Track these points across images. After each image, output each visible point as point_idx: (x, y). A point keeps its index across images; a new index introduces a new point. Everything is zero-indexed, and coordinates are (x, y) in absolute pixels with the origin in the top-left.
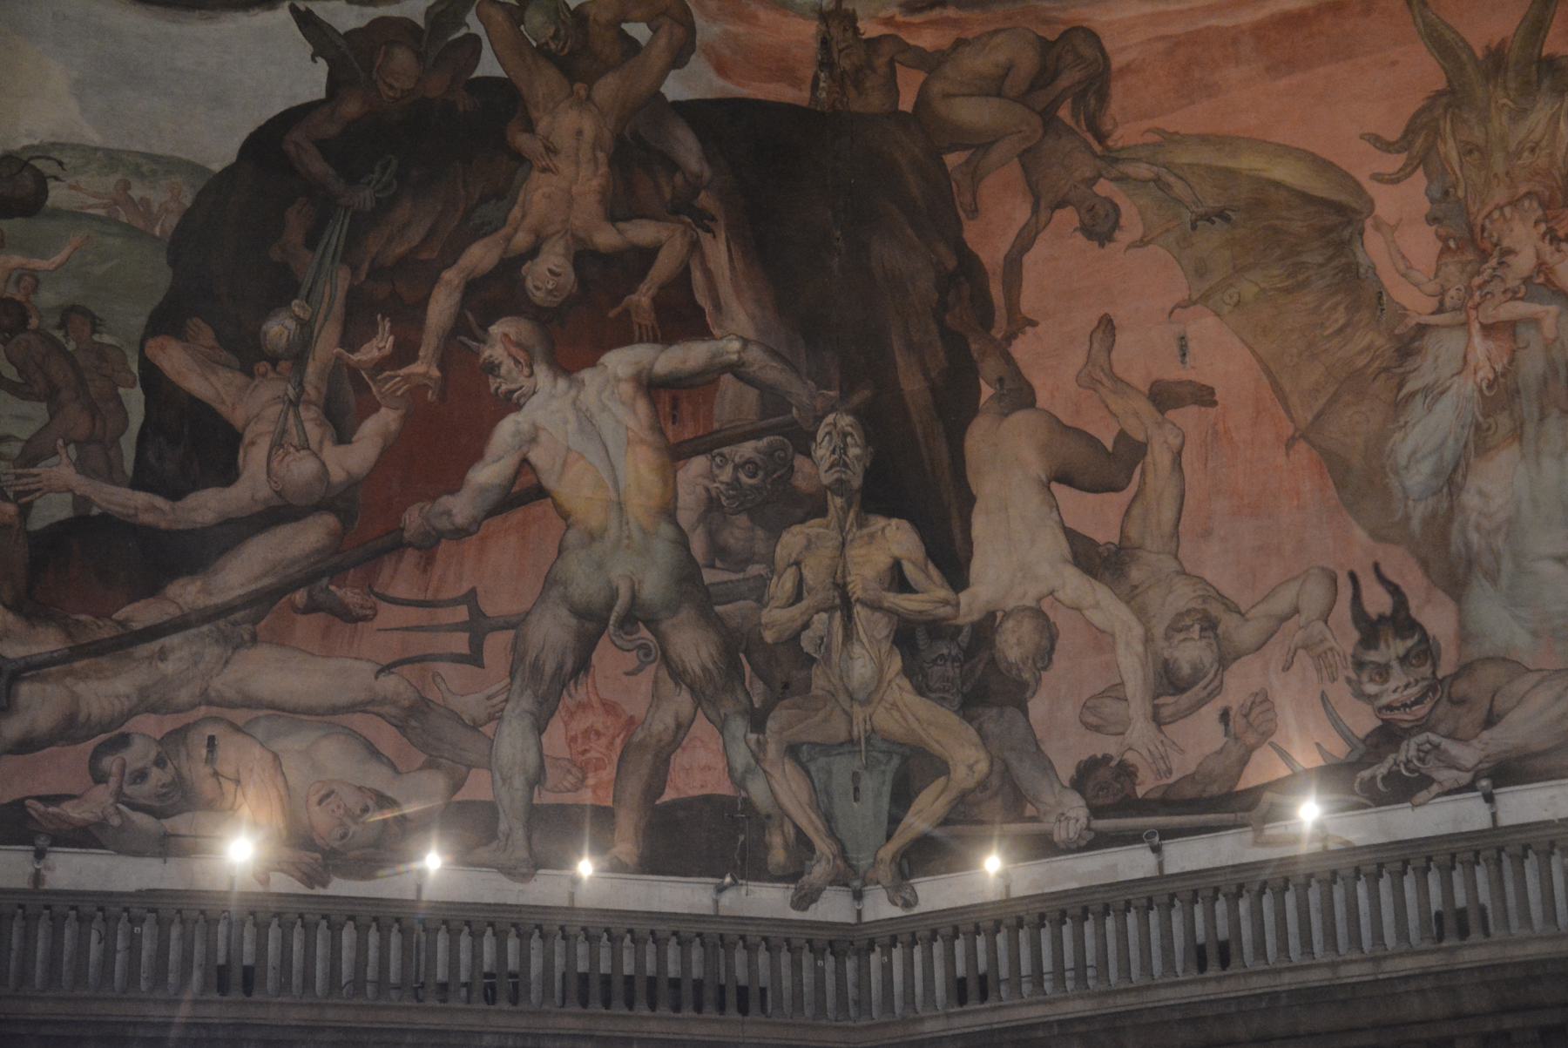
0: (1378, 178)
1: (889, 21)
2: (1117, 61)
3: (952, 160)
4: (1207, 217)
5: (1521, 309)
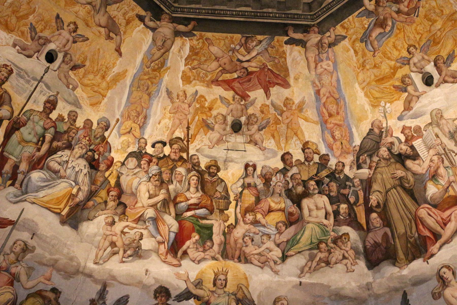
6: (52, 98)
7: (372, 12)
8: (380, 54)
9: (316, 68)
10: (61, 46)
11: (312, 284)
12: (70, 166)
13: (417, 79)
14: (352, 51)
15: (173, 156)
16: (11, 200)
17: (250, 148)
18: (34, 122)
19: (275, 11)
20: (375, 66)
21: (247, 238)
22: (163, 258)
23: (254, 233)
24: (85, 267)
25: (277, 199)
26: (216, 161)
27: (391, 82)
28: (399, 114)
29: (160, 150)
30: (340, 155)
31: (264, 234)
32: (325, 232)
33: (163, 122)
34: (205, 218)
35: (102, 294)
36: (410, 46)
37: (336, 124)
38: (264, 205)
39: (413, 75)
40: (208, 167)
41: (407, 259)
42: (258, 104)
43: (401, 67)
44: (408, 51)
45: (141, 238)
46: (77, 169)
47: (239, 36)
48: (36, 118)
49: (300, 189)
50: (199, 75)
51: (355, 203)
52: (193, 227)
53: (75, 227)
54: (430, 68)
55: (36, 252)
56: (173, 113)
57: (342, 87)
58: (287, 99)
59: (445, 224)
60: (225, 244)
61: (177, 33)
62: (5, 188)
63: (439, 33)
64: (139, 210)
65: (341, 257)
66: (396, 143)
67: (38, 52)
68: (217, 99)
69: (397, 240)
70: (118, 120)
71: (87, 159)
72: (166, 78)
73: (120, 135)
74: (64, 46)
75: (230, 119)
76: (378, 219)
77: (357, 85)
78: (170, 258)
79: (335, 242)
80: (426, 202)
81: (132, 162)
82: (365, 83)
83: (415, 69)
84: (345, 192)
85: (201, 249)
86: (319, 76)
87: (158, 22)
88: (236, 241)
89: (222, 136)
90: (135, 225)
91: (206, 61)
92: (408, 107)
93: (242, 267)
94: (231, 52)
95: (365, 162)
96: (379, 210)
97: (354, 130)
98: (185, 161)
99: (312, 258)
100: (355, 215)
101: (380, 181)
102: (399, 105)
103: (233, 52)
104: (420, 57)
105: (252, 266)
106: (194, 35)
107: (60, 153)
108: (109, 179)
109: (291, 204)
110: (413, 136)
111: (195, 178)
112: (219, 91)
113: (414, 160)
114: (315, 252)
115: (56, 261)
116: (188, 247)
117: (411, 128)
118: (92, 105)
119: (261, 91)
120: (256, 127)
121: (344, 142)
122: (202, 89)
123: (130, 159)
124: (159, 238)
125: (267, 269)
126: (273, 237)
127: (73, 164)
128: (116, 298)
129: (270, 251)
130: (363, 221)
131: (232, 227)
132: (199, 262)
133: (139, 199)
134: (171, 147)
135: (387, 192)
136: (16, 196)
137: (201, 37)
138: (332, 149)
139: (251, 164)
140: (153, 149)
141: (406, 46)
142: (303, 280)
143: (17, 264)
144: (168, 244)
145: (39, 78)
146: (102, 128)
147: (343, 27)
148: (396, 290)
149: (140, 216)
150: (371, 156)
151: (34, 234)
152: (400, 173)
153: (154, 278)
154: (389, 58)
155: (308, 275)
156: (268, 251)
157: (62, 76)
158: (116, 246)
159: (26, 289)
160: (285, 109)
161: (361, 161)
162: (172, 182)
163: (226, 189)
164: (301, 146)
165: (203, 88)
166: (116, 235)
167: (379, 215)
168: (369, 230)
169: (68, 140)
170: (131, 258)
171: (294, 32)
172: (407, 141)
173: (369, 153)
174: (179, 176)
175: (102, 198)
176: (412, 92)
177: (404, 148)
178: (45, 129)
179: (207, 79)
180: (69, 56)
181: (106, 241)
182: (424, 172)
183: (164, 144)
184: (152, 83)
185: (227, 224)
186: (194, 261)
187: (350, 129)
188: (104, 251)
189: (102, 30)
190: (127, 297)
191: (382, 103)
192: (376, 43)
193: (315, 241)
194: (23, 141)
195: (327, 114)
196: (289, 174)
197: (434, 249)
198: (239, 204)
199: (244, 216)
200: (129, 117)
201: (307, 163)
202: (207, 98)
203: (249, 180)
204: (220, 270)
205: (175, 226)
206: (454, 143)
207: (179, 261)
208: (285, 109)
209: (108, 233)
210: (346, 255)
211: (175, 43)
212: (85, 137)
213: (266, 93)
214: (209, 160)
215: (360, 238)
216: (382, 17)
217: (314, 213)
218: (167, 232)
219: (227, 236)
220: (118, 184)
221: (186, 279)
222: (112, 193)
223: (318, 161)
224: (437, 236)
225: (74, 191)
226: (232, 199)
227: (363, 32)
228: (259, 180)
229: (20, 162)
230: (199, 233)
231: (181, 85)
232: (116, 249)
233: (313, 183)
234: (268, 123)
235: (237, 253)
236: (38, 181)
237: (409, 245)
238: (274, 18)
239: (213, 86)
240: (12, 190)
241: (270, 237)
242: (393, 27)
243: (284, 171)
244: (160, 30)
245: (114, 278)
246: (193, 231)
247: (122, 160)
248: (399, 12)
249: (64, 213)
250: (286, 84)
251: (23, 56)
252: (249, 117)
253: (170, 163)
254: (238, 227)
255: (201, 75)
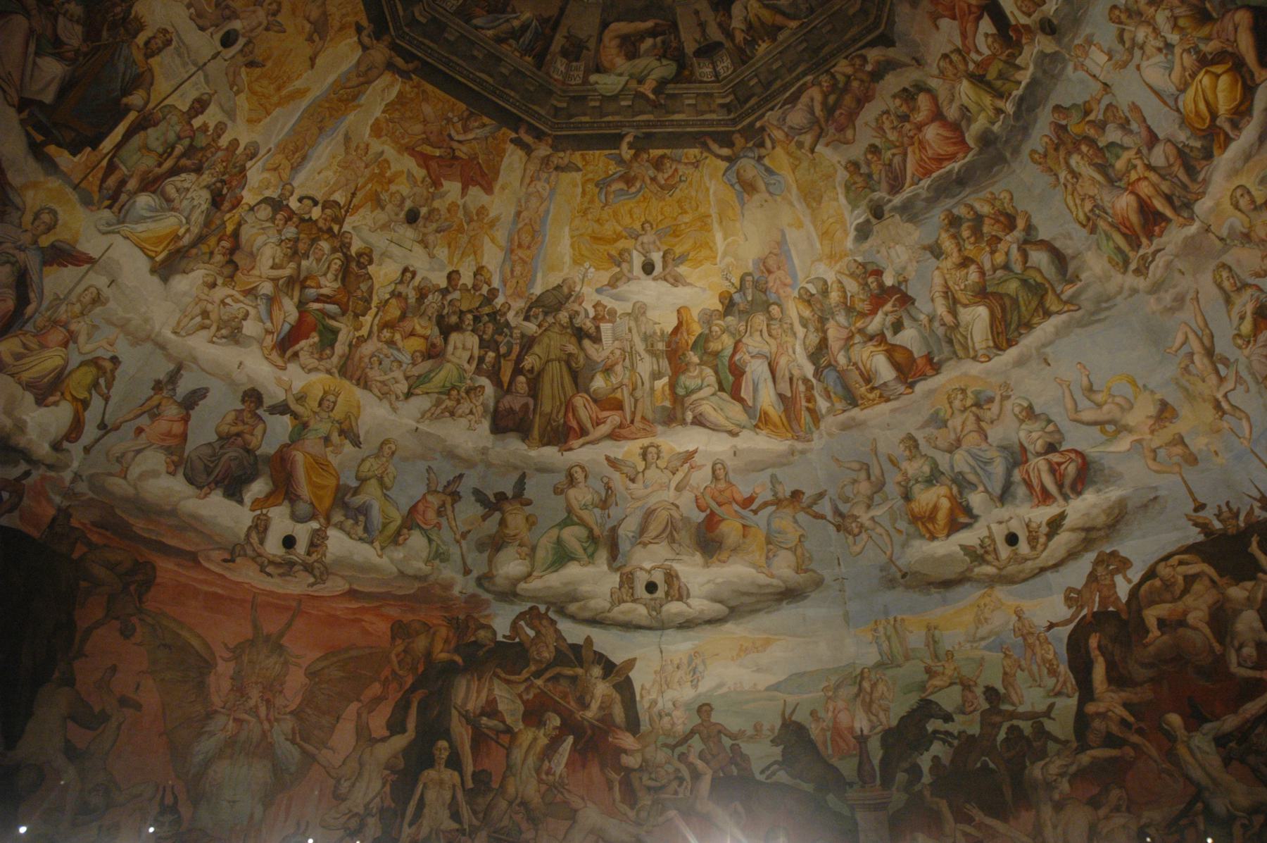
0: (221, 657)
1: (84, 525)
2: (158, 580)
3: (83, 584)
4: (165, 646)
5: (246, 716)
6: (205, 97)
7: (625, 162)
8: (610, 211)
9: (529, 184)
10: (248, 28)
11: (429, 434)
12: (189, 196)
13: (638, 260)
14: (580, 190)
15: (321, 224)
16: (101, 228)
17: (418, 249)
18: (169, 124)
19: (518, 98)
20: (598, 221)
21: (375, 358)
22: (266, 352)
23: (386, 356)
24: (159, 334)
25: (424, 322)
26: (371, 251)
27: (607, 248)
28: (599, 286)
29: (307, 208)
30: (510, 296)
31: (396, 360)
32: (462, 379)
33: (325, 174)
34: (333, 318)
35: (174, 377)
36: (647, 221)
37: (520, 258)
38: (407, 325)
39: (635, 253)
40: (360, 255)
41: (541, 441)
42: (450, 199)
43: (626, 238)
44: (642, 225)
45: (246, 315)
46: (195, 203)
47: (464, 107)
48: (174, 119)
49: (454, 319)
50: (393, 133)
51: (505, 356)
52: (316, 325)
53: (165, 279)
54: (657, 257)
55: (108, 305)
56: (343, 167)
57: (549, 221)
58: (483, 207)
59: (598, 423)
60: (347, 358)
61: (390, 66)
62: (99, 209)
63: (683, 227)
64: (253, 280)
65: (467, 411)
66: (582, 314)
67: (217, 26)
68: (403, 172)
69: (537, 417)
70: (270, 150)
71: (212, 192)
72: (351, 117)
73: (265, 169)
74: (252, 30)
75: (408, 204)
76: (525, 385)
77: (567, 229)
78: (275, 356)
79: (468, 392)
80: (587, 392)
81: (265, 212)
82: (576, 233)
83: (639, 248)
84: (499, 338)
85: (316, 356)
86: (529, 195)
87: (375, 42)
88: (361, 358)
89: (391, 221)
90: (242, 298)
91: (411, 118)
92: (613, 283)
93: (359, 393)
94: (445, 122)
95: (536, 317)
96: (529, 376)
97: (539, 275)
98: (333, 235)
99: (438, 403)
100: (500, 368)
101: (545, 346)
102: (604, 277)
103: (448, 123)
104: (652, 240)
105: (370, 394)
106: (411, 79)
107: (184, 176)
108: (227, 224)
109: (438, 333)
110: (604, 317)
111: (339, 262)
112: (409, 163)
113: (594, 343)
114: (444, 397)
115: (129, 320)
116: (302, 349)
117: (606, 307)
118: (250, 121)
119: (459, 185)
120: (434, 226)
121: (521, 281)
122: (390, 152)
123: (263, 205)
124: (269, 325)
125: (385, 403)
126: (404, 366)
127: (194, 195)
128: (192, 387)
129: (396, 382)
130: (506, 379)
131: (362, 340)
132: (310, 371)
133: (258, 264)
134: (323, 210)
135: (548, 361)
136: (109, 224)
137: (418, 86)
138: (505, 285)
139: (411, 269)
140: (299, 204)
141: (643, 219)
142: (421, 427)
143: (79, 319)
144: (278, 336)
145: (201, 64)
146: (247, 155)
147: (583, 156)
148: (516, 468)
149: (253, 289)
150: (546, 314)
151: (113, 281)
152: (572, 348)
153: (248, 376)
154: (618, 222)
155: (427, 422)
156: (393, 381)
157: (232, 70)
158: (208, 318)
159: (81, 353)
160: (475, 218)
161: (532, 313)
162: (308, 257)
163: (371, 289)
164: (475, 269)
165: (392, 151)
166: (212, 303)
167: (529, 382)
168: (509, 391)
169: (200, 161)
170: (224, 340)
171: (526, 132)
172: (595, 318)
173: (546, 310)
174: (320, 253)
175: (209, 246)
176: (625, 271)
177: (589, 325)
178: (179, 138)
179: (403, 142)
180: (251, 45)
181: (198, 307)
182: (599, 360)
183: (316, 203)
184: (331, 116)
185: (357, 334)
186: (303, 368)
187: (536, 273)
188: (192, 319)
189: (308, 26)
190: (207, 390)
191: (587, 265)
192: (612, 196)
193: (448, 384)
194: (146, 148)
195: (516, 243)
196: (449, 298)
197: (575, 443)
198: (380, 313)
199: (380, 331)
200: (284, 149)
201: (472, 292)
202: (392, 165)
203: (401, 288)
204: (332, 388)
205: (293, 315)
206: (644, 347)
207: (285, 363)
208: (475, 218)
209: (205, 297)
210: (474, 410)
211: (383, 77)
212: (223, 161)
213: (463, 189)
214: (364, 245)
215: (495, 397)
216: (633, 174)
217: (459, 352)
218: (281, 321)
219: (353, 349)
220: (236, 234)
221: (287, 388)
222: (223, 243)
223: (485, 294)
224: (583, 432)
225: (182, 231)
226: (373, 305)
227: (603, 176)
228: (414, 293)
229: (131, 176)
230: (321, 335)
231: (367, 136)
232: (207, 322)
233: (470, 316)
234: (450, 227)
235: (358, 373)
236: (143, 209)
237: (549, 428)
238: (512, 104)
239: (406, 155)
240: (107, 214)
241: (401, 366)
242: (639, 191)
243: (444, 292)
244: (372, 52)
245: (195, 360)
246: (314, 329)
247: (252, 203)
248: (653, 179)
249: (158, 259)
250: (489, 190)
251: (194, 26)
252: (432, 211)
253: (314, 231)
254: (370, 342)
255: (398, 133)
